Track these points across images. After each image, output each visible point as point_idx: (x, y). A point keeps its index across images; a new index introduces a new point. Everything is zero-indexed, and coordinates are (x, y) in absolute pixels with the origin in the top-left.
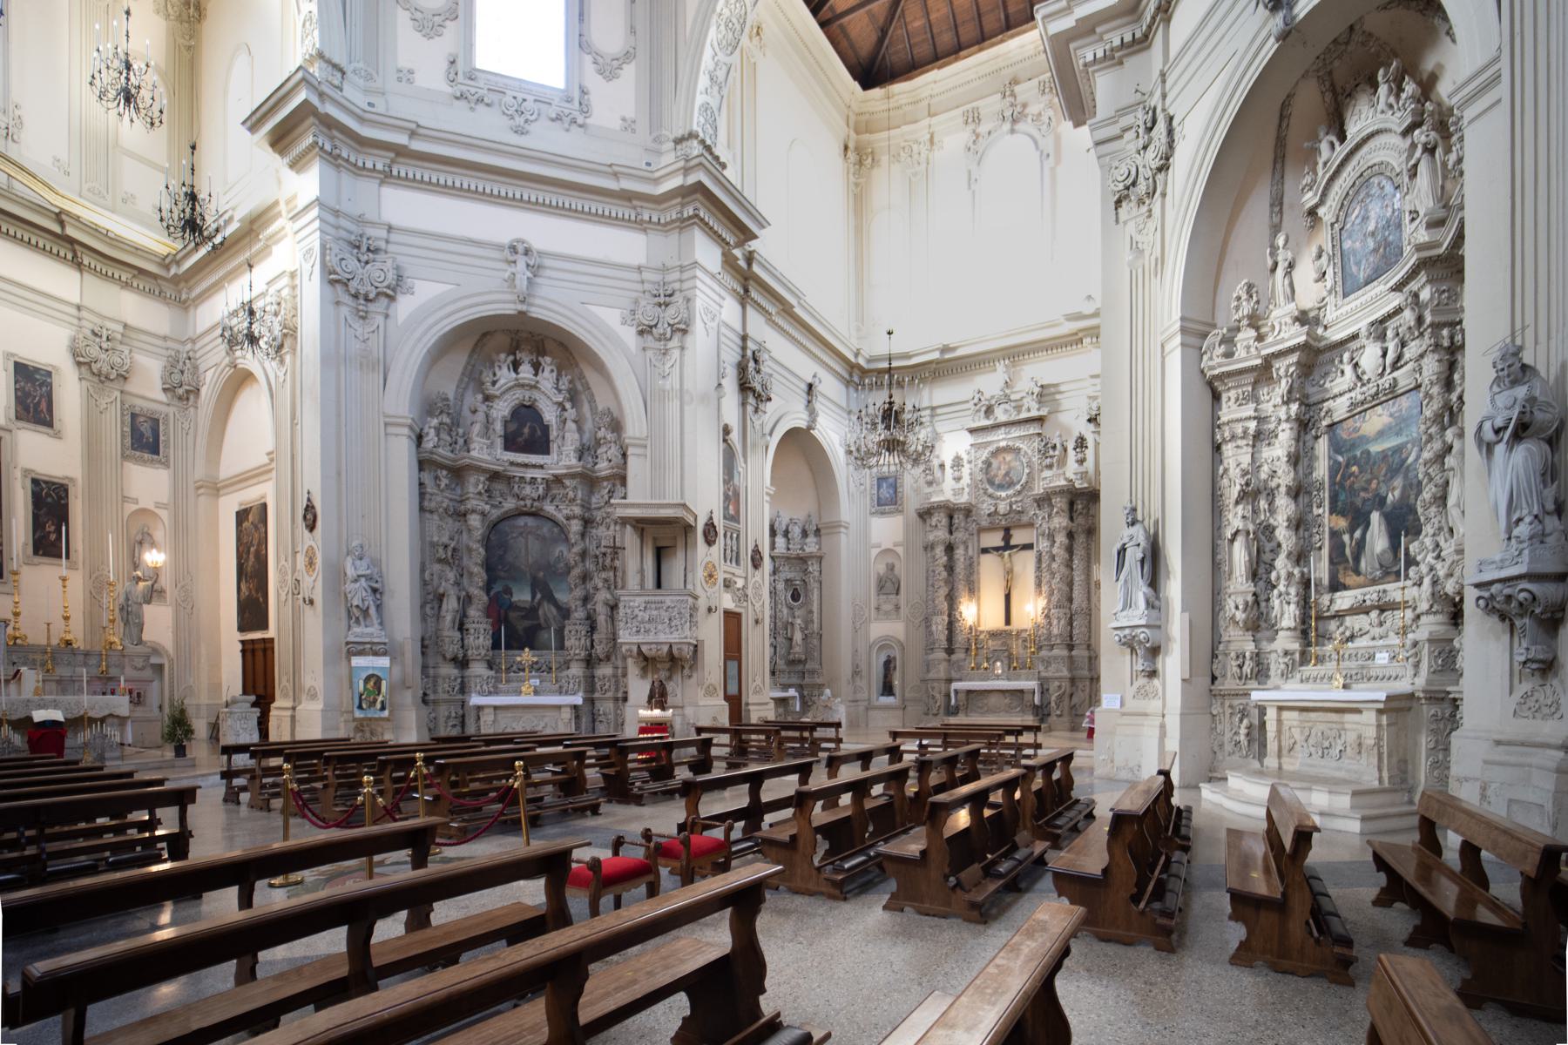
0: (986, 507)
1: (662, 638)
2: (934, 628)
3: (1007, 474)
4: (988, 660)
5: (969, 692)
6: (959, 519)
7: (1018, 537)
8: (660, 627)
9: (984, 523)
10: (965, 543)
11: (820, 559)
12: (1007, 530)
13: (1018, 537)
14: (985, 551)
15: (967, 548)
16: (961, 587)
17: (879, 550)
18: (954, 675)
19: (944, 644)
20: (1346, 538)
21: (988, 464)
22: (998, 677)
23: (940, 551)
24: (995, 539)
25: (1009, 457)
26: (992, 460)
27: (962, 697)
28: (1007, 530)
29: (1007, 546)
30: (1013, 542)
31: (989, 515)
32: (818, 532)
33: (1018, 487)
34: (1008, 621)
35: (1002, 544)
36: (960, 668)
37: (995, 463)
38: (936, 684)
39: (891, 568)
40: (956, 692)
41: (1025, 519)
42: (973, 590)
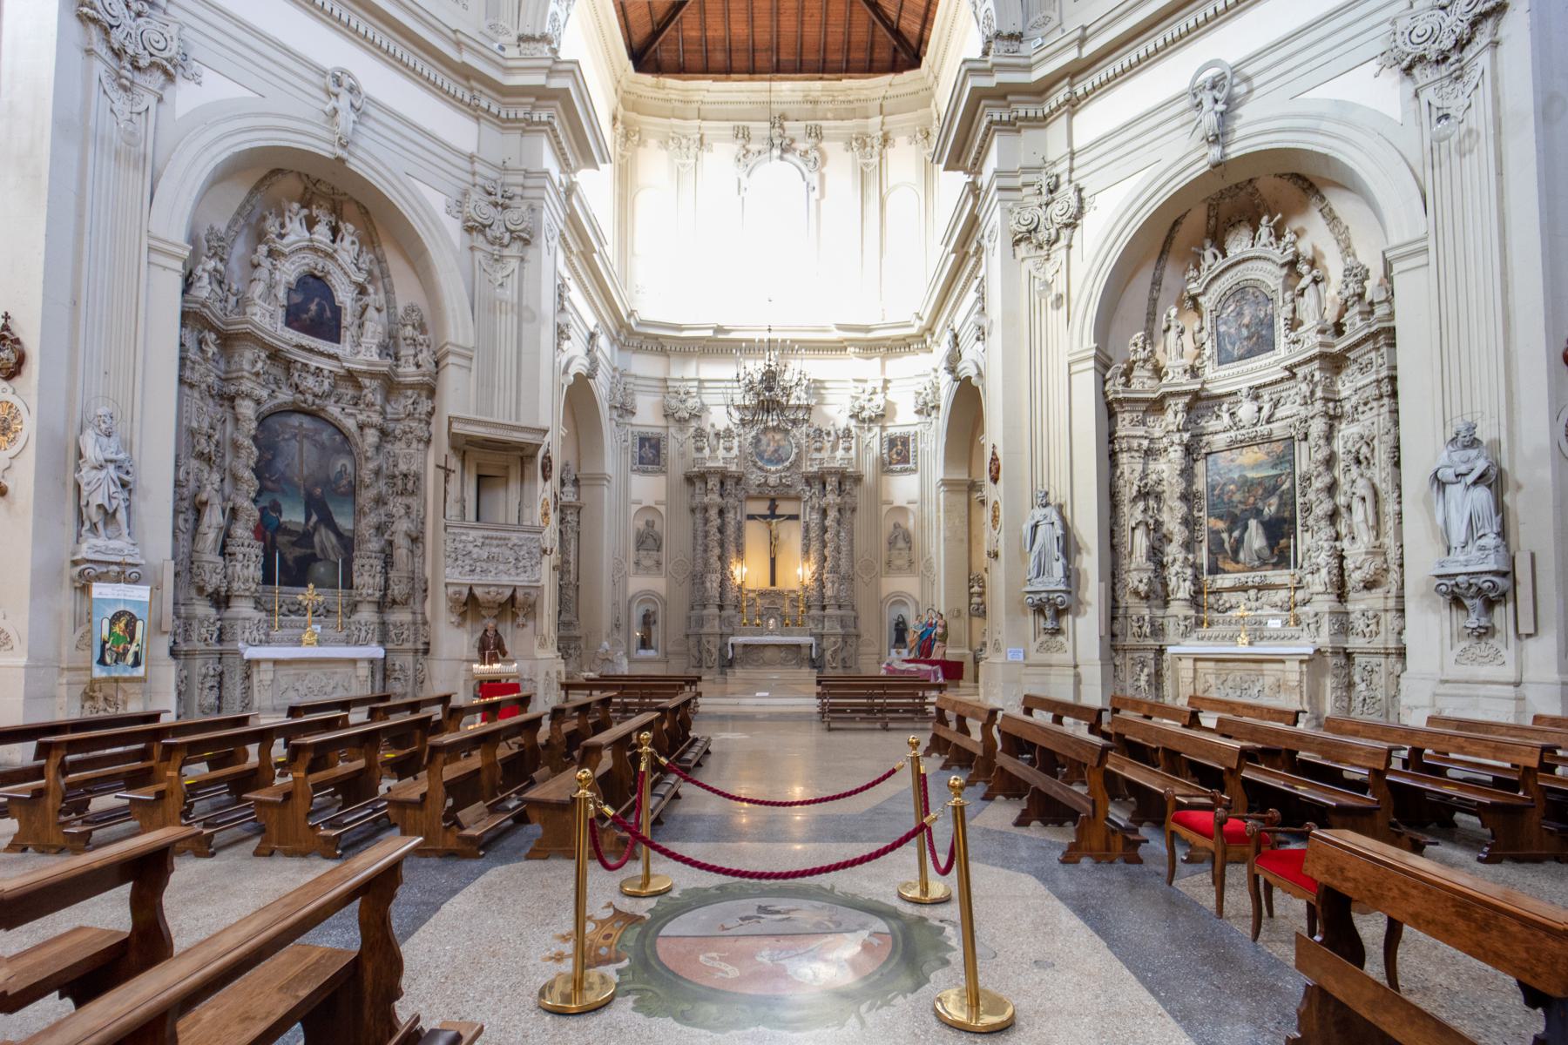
1: (505, 580)
2: (708, 585)
4: (761, 616)
5: (745, 646)
6: (729, 484)
7: (784, 508)
8: (501, 567)
10: (735, 508)
11: (579, 510)
12: (773, 500)
13: (784, 508)
14: (751, 517)
16: (732, 548)
17: (639, 507)
18: (726, 630)
22: (772, 633)
23: (713, 513)
24: (761, 508)
27: (739, 650)
28: (773, 500)
29: (773, 515)
32: (576, 482)
34: (773, 583)
35: (768, 513)
36: (730, 624)
38: (711, 639)
39: (650, 524)
41: (792, 493)
42: (740, 553)
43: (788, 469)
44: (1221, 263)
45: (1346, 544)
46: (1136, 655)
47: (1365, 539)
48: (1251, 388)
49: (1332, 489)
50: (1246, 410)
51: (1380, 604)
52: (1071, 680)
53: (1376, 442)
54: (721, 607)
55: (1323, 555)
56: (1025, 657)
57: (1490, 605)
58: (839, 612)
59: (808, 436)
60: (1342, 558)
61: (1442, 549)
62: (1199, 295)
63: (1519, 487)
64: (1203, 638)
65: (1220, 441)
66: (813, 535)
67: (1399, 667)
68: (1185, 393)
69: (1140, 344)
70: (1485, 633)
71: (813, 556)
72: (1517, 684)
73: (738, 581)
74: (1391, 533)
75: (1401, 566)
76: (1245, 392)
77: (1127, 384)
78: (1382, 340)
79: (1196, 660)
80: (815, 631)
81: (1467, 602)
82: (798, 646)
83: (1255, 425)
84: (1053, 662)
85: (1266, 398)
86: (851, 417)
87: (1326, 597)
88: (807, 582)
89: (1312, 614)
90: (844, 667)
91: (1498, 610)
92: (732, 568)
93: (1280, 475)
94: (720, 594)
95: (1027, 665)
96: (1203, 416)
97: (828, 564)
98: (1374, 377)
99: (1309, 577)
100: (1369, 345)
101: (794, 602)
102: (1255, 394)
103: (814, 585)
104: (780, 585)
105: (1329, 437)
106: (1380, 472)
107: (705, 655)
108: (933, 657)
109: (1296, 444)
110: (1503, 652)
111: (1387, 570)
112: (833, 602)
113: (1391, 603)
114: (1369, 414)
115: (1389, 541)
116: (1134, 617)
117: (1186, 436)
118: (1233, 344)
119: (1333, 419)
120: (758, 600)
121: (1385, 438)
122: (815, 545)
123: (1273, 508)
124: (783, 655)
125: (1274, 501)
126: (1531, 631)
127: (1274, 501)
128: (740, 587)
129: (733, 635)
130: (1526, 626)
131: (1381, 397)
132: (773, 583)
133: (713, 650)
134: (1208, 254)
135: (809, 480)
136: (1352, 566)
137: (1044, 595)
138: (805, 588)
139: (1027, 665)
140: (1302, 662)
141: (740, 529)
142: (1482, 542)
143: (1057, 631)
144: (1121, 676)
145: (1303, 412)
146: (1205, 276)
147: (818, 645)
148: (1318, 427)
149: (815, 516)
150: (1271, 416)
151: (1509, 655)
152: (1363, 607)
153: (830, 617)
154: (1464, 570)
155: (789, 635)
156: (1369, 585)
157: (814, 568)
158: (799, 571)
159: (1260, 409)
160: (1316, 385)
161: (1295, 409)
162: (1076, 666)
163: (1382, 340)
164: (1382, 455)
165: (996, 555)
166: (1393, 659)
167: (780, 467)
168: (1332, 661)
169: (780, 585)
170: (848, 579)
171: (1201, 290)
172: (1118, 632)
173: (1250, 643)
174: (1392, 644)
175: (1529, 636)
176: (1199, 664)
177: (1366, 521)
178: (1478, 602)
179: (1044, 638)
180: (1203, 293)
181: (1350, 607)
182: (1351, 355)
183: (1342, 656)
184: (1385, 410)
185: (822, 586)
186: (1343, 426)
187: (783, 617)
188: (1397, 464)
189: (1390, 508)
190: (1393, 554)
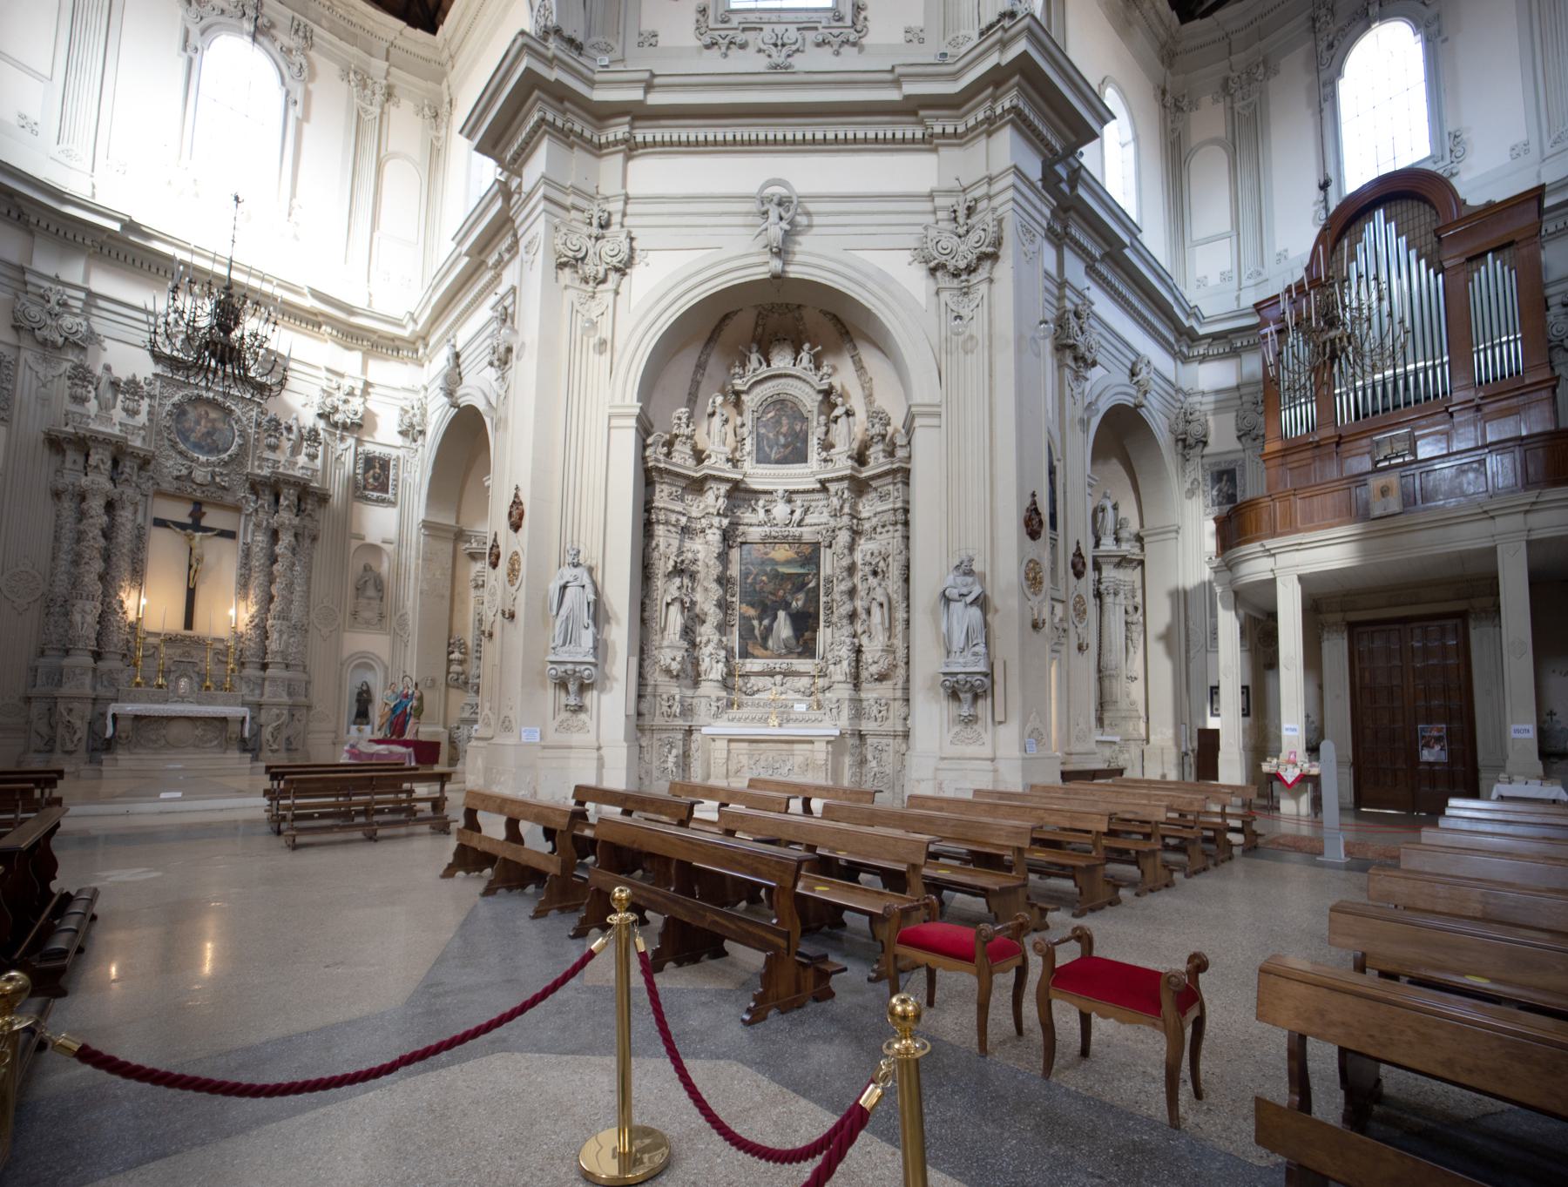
0: (172, 465)
2: (77, 618)
3: (209, 434)
4: (166, 673)
5: (137, 718)
7: (212, 518)
9: (165, 486)
12: (198, 504)
13: (212, 518)
15: (135, 512)
16: (124, 565)
18: (101, 691)
19: (92, 645)
20: (756, 623)
21: (180, 411)
22: (182, 699)
24: (181, 513)
25: (213, 415)
26: (189, 408)
28: (198, 504)
29: (196, 526)
30: (205, 522)
31: (177, 478)
33: (225, 456)
34: (189, 622)
35: (189, 521)
36: (113, 683)
37: (192, 414)
38: (76, 705)
40: (114, 716)
41: (229, 499)
42: (138, 575)
43: (226, 464)
44: (764, 371)
45: (864, 640)
46: (664, 736)
47: (880, 639)
48: (786, 491)
49: (852, 593)
50: (780, 510)
51: (889, 694)
52: (594, 764)
53: (890, 559)
54: (97, 656)
55: (844, 649)
56: (541, 739)
57: (976, 697)
58: (286, 674)
59: (258, 425)
60: (858, 651)
61: (943, 652)
62: (743, 392)
63: (996, 611)
64: (733, 720)
65: (755, 533)
66: (255, 563)
67: (904, 747)
68: (727, 480)
69: (684, 420)
70: (970, 720)
71: (253, 594)
72: (993, 760)
73: (132, 617)
74: (900, 636)
75: (907, 663)
76: (780, 493)
77: (668, 455)
78: (899, 477)
79: (730, 741)
80: (249, 698)
81: (961, 696)
82: (224, 720)
83: (787, 525)
84: (573, 744)
85: (799, 503)
86: (320, 416)
87: (845, 685)
88: (242, 628)
89: (834, 700)
90: (288, 750)
91: (980, 703)
92: (123, 595)
93: (808, 574)
94: (99, 634)
95: (544, 747)
96: (739, 507)
97: (276, 606)
98: (891, 506)
99: (832, 667)
100: (889, 479)
101: (221, 655)
102: (790, 496)
103: (252, 633)
104: (201, 627)
105: (851, 548)
106: (894, 583)
107: (61, 731)
108: (408, 736)
109: (822, 549)
110: (983, 735)
111: (895, 666)
112: (279, 659)
113: (899, 694)
114: (885, 536)
115: (898, 642)
116: (665, 696)
117: (725, 522)
118: (771, 448)
119: (856, 533)
120: (163, 649)
121: (898, 557)
122: (257, 579)
123: (800, 603)
124: (199, 732)
125: (801, 596)
126: (1002, 719)
127: (801, 596)
128: (133, 627)
129: (116, 700)
130: (999, 718)
131: (895, 524)
132: (189, 622)
133: (78, 723)
134: (754, 357)
135: (256, 486)
136: (870, 661)
137: (570, 667)
138: (239, 637)
139: (544, 747)
141: (140, 538)
142: (976, 649)
143: (580, 708)
144: (647, 757)
145: (832, 523)
146: (750, 378)
147: (252, 718)
148: (843, 537)
149: (261, 539)
150: (802, 520)
151: (987, 737)
152: (875, 695)
153: (273, 680)
155: (209, 704)
156: (882, 678)
157: (253, 609)
158: (232, 612)
159: (792, 512)
160: (844, 501)
161: (825, 518)
162: (599, 748)
163: (899, 477)
164: (895, 571)
165: (512, 616)
166: (899, 740)
167: (213, 459)
169: (201, 627)
170: (302, 629)
171: (745, 388)
172: (645, 711)
173: (780, 725)
174: (900, 728)
175: (1000, 723)
176: (733, 745)
177: (883, 623)
178: (969, 696)
179: (564, 715)
180: (747, 392)
181: (863, 695)
182: (874, 484)
183: (857, 737)
184: (898, 534)
185: (265, 635)
186: (862, 541)
187: (202, 677)
188: (907, 580)
189: (900, 615)
190: (901, 653)
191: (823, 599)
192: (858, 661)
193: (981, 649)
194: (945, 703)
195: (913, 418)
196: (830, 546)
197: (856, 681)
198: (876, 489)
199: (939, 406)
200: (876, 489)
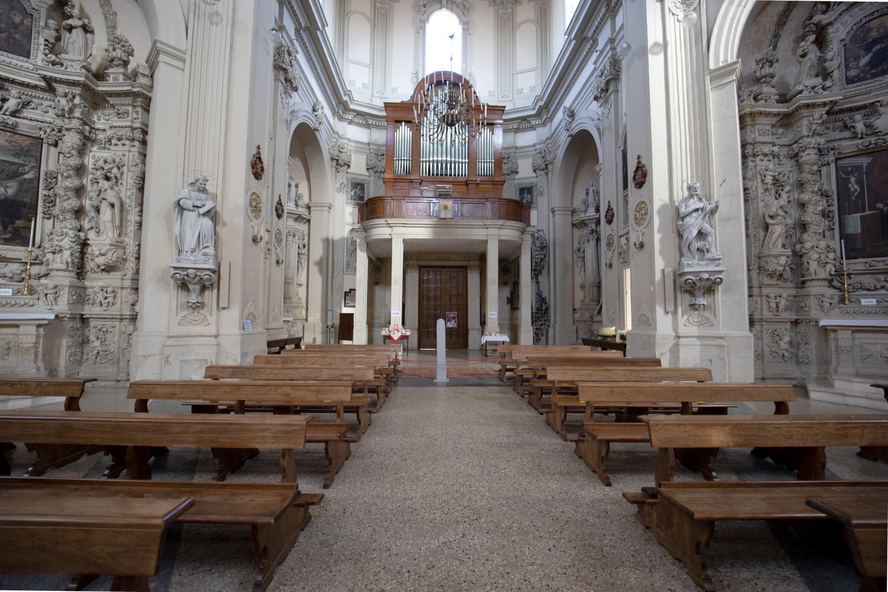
45: (92, 235)
47: (109, 235)
49: (79, 191)
51: (118, 283)
53: (125, 169)
55: (66, 240)
57: (204, 288)
60: (84, 244)
61: (175, 251)
63: (225, 224)
67: (131, 328)
74: (131, 235)
75: (138, 258)
78: (139, 101)
81: (190, 287)
87: (66, 273)
93: (23, 165)
98: (129, 124)
99: (50, 256)
100: (129, 100)
106: (127, 189)
109: (45, 146)
111: (125, 260)
113: (128, 283)
114: (120, 148)
115: (130, 241)
121: (133, 169)
131: (133, 140)
136: (97, 253)
140: (39, 326)
142: (206, 250)
145: (59, 122)
148: (71, 139)
152: (101, 284)
154: (194, 266)
156: (109, 269)
160: (75, 106)
161: (50, 116)
163: (139, 101)
164: (129, 179)
166: (126, 323)
168: (68, 325)
174: (127, 312)
177: (113, 221)
178: (198, 287)
181: (87, 283)
182: (112, 100)
183: (78, 321)
184: (135, 149)
186: (95, 149)
188: (141, 189)
189: (133, 217)
190: (131, 249)
191: (42, 192)
192: (83, 253)
193: (211, 251)
194: (174, 292)
195: (158, 53)
196: (56, 145)
197: (80, 271)
198: (113, 106)
199: (185, 53)
200: (113, 106)
